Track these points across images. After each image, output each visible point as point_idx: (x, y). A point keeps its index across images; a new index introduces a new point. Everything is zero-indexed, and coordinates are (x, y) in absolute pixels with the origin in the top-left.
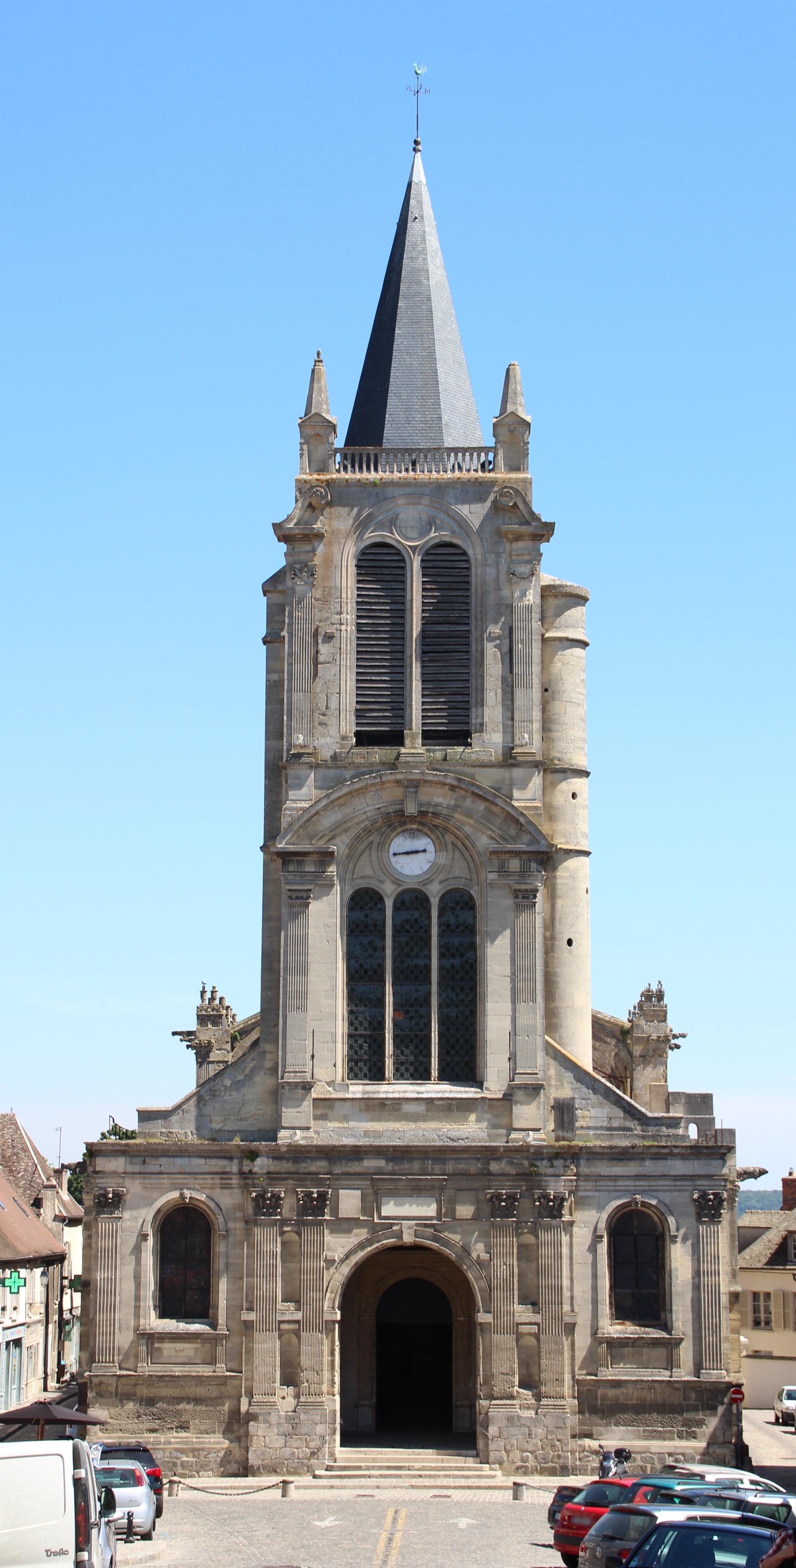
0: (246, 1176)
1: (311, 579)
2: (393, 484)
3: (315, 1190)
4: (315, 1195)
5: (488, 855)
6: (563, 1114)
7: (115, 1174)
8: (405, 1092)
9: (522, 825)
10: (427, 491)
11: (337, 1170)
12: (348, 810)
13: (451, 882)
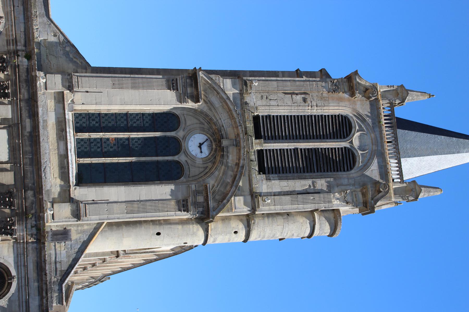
0: (16, 53)
1: (332, 91)
2: (381, 131)
3: (10, 91)
4: (7, 91)
5: (204, 184)
6: (62, 234)
8: (71, 142)
9: (222, 202)
10: (380, 148)
12: (220, 110)
13: (187, 167)
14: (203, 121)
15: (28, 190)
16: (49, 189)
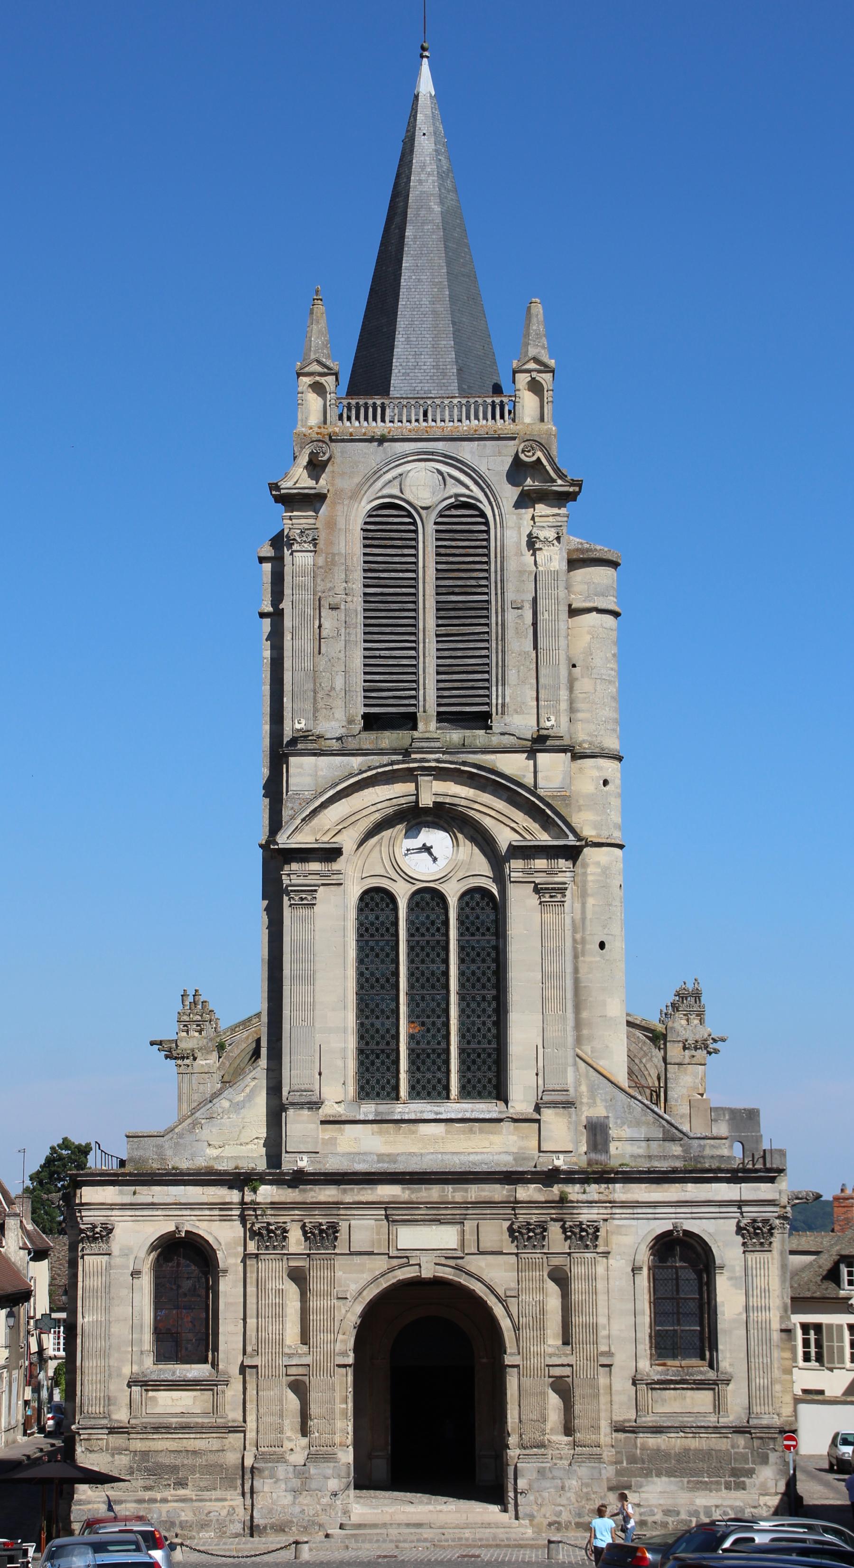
6: (595, 1135)
7: (102, 1206)
8: (421, 1112)
11: (348, 1198)
16: (510, 1158)
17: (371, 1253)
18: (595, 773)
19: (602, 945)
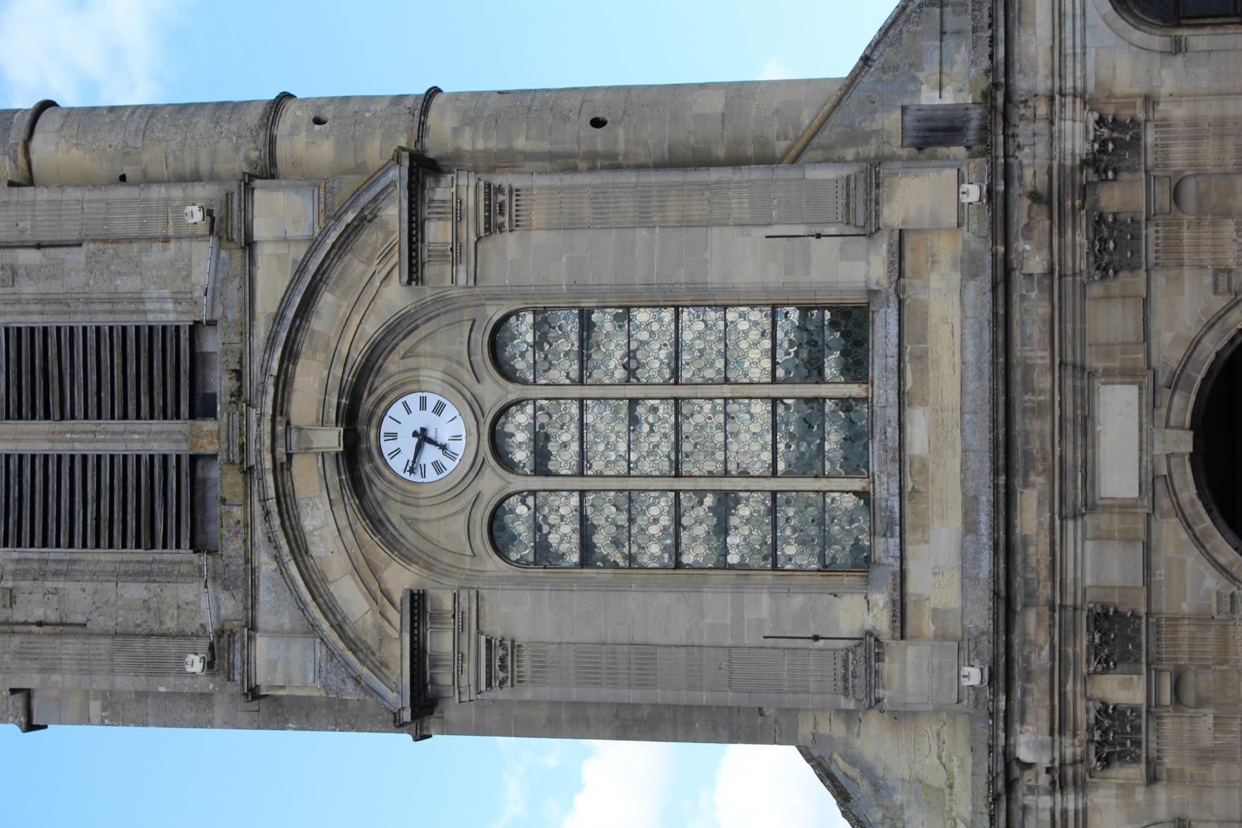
13: (477, 359)
14: (404, 529)
15: (1043, 275)
16: (972, 286)
17: (1147, 548)
18: (301, 139)
19: (597, 123)
